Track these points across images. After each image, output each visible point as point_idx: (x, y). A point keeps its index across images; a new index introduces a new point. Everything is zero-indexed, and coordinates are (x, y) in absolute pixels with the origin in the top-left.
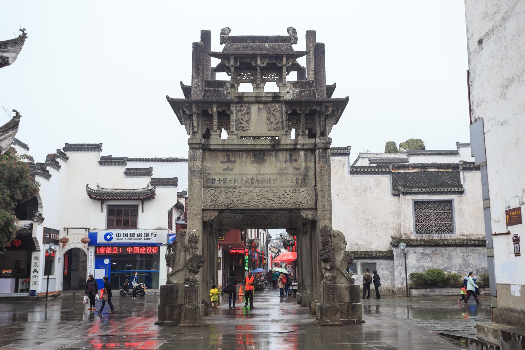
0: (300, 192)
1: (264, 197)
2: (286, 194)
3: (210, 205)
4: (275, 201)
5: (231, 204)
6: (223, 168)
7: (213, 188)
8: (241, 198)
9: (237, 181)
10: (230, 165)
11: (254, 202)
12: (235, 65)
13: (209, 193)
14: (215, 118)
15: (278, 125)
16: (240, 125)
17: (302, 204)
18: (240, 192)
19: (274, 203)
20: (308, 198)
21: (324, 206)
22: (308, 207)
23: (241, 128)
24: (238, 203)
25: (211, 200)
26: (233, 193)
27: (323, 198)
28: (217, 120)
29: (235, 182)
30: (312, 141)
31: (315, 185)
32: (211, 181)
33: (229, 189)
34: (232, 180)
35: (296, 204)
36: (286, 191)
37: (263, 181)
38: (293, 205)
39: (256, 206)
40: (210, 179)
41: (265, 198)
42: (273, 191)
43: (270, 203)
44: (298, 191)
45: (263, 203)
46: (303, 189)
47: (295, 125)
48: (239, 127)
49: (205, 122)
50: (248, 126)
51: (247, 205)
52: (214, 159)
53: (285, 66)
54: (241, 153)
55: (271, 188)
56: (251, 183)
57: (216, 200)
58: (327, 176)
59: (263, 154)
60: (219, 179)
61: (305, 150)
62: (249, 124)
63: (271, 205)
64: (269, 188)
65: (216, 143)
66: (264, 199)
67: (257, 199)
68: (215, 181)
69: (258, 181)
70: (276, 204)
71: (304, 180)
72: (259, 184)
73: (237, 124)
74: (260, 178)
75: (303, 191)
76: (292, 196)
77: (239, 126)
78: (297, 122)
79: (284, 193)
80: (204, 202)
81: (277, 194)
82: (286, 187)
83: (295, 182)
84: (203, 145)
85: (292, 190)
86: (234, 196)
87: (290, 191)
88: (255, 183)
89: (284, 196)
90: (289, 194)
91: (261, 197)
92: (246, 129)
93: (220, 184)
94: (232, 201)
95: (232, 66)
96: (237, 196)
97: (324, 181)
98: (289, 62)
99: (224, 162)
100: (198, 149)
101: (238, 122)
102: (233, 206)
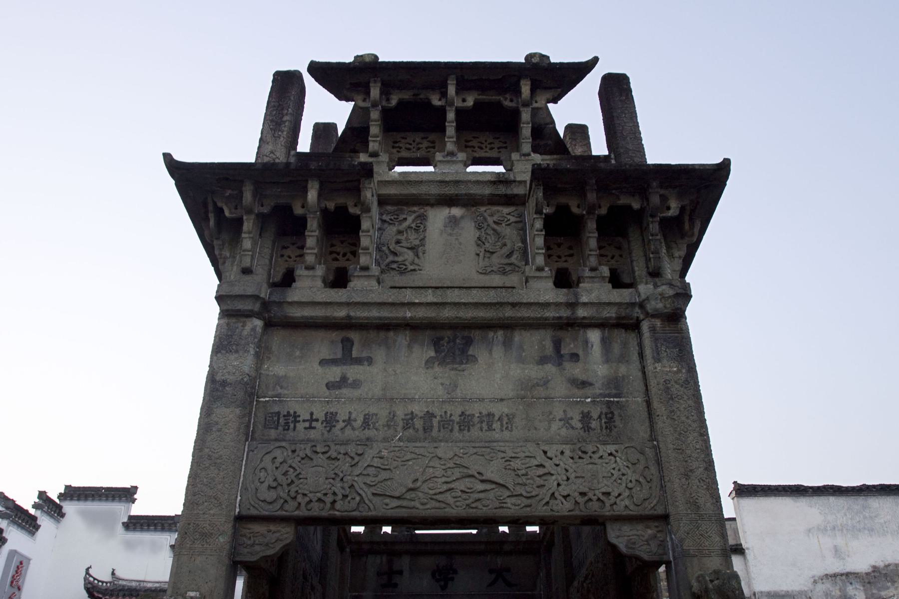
0: (601, 457)
1: (470, 472)
2: (548, 463)
3: (269, 500)
4: (510, 486)
5: (345, 496)
6: (326, 381)
7: (283, 444)
8: (384, 475)
9: (374, 423)
10: (353, 372)
11: (431, 492)
12: (384, 103)
13: (268, 458)
14: (313, 226)
15: (513, 259)
16: (391, 258)
17: (613, 500)
18: (381, 458)
19: (508, 493)
20: (631, 476)
21: (695, 506)
22: (634, 511)
23: (394, 266)
24: (374, 494)
25: (275, 484)
26: (357, 459)
27: (687, 476)
28: (317, 233)
29: (366, 424)
30: (623, 295)
31: (653, 437)
32: (282, 421)
33: (343, 447)
34: (355, 420)
35: (590, 500)
36: (549, 454)
37: (466, 422)
38: (577, 503)
39: (438, 505)
40: (278, 413)
41: (473, 476)
42: (503, 455)
43: (491, 495)
44: (594, 453)
45: (464, 496)
46: (611, 448)
47: (566, 261)
48: (388, 265)
49: (287, 252)
50: (417, 261)
51: (405, 503)
52: (298, 353)
53: (526, 105)
54: (391, 334)
55: (495, 444)
56: (421, 429)
57: (292, 482)
58: (690, 402)
59: (463, 338)
60: (312, 414)
61: (601, 325)
62: (421, 254)
63: (497, 504)
64: (487, 444)
65: (310, 300)
66: (467, 480)
67: (444, 479)
68: (296, 421)
69: (446, 423)
70: (513, 500)
71: (609, 419)
72: (451, 431)
73: (381, 257)
74: (455, 411)
75: (610, 454)
76: (571, 470)
77: (388, 260)
78: (571, 252)
79: (541, 459)
80: (245, 489)
81: (516, 464)
82: (550, 442)
83: (579, 425)
84: (266, 305)
85: (573, 451)
86: (357, 471)
87: (562, 453)
88: (435, 430)
89: (541, 471)
90: (562, 464)
91: (457, 473)
92: (412, 267)
93: (313, 431)
94: (352, 486)
95: (374, 105)
96: (371, 471)
97: (684, 419)
98: (538, 99)
99: (334, 362)
100: (249, 315)
101: (387, 252)
102: (354, 504)
